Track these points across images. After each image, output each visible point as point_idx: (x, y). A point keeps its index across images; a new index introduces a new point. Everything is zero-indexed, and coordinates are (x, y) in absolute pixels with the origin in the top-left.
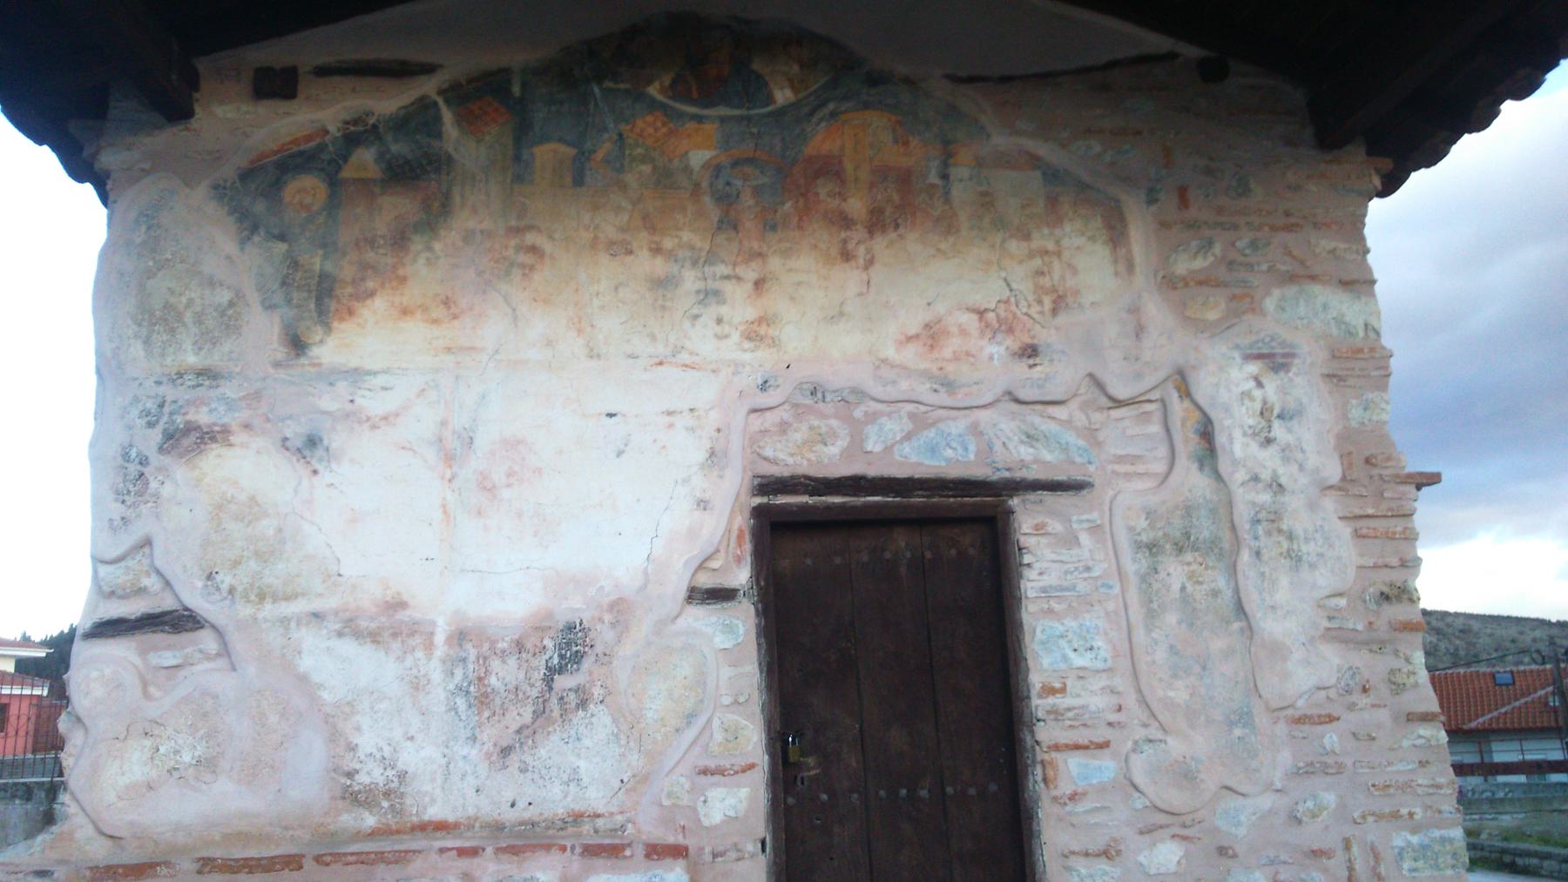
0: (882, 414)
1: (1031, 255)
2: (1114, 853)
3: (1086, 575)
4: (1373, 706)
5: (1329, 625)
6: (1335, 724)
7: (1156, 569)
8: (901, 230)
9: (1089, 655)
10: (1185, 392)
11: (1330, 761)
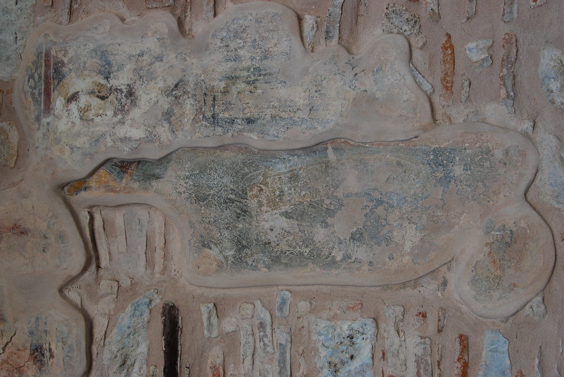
3: (268, 330)
5: (336, 39)
6: (454, 41)
7: (265, 244)
9: (358, 340)
11: (500, 53)
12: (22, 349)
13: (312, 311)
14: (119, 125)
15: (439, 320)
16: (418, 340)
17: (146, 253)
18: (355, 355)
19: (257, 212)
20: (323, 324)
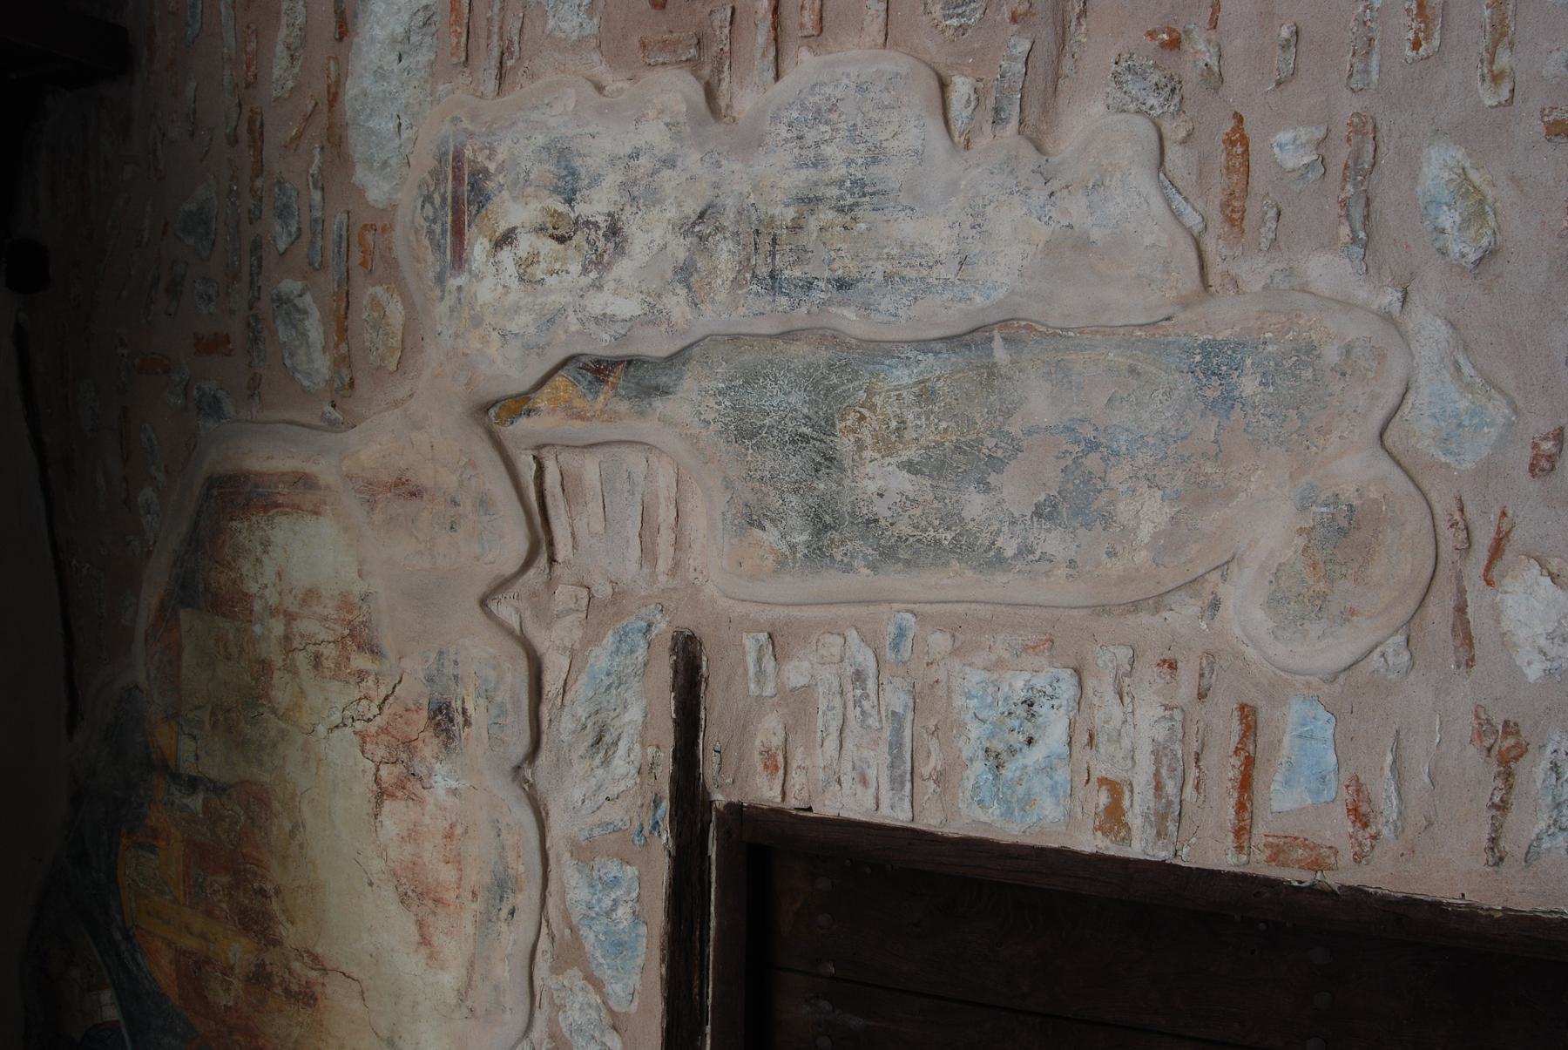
0: (552, 1022)
1: (293, 671)
2: (1511, 741)
3: (871, 685)
4: (1214, 24)
6: (1248, 128)
7: (868, 522)
8: (269, 887)
9: (1043, 708)
10: (518, 405)
11: (1342, 154)
12: (414, 708)
13: (954, 652)
14: (591, 292)
15: (1202, 675)
16: (1160, 712)
17: (640, 537)
18: (1036, 737)
19: (853, 460)
20: (975, 677)
